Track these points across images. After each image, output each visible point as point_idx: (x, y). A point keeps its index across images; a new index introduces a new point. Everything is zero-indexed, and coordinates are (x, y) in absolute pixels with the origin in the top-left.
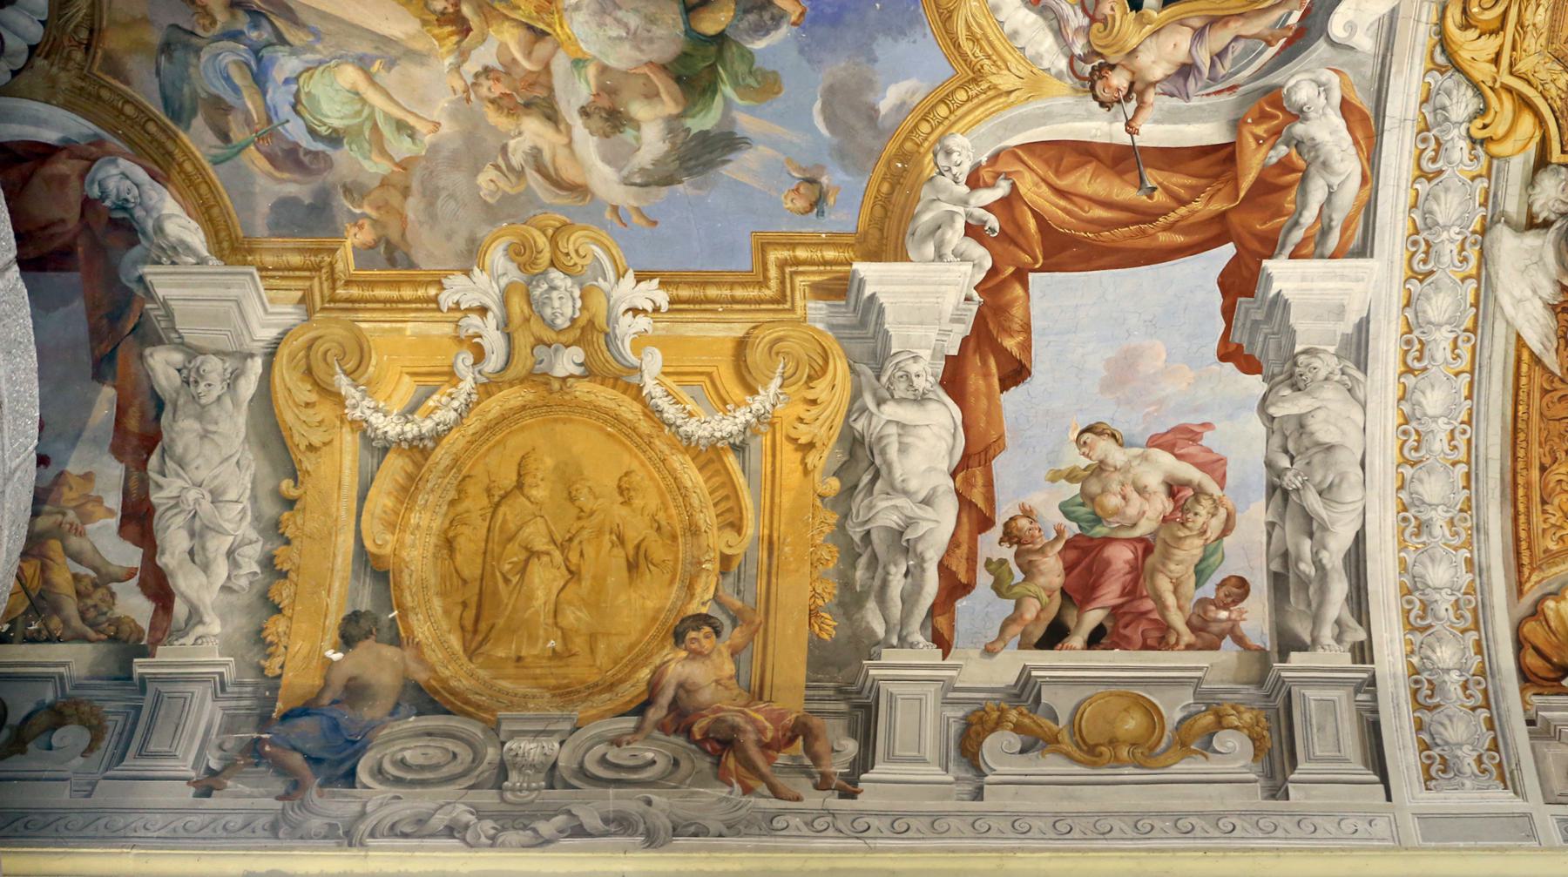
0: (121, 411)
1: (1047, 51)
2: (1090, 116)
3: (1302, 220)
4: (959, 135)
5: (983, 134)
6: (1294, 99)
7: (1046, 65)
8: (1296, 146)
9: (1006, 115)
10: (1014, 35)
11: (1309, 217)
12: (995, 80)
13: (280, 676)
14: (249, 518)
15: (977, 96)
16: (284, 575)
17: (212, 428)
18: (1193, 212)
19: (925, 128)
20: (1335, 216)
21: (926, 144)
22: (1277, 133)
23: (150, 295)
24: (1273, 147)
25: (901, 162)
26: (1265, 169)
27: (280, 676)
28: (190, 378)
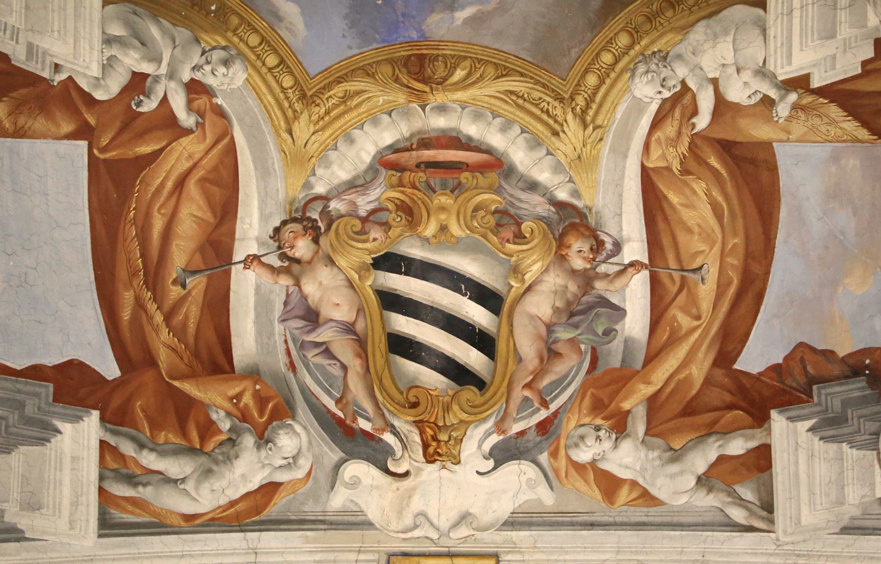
1: (333, 173)
3: (145, 452)
4: (245, 76)
5: (246, 102)
6: (281, 432)
7: (320, 172)
8: (230, 439)
9: (267, 129)
10: (351, 141)
11: (150, 460)
12: (304, 117)
15: (287, 98)
19: (254, 40)
20: (149, 489)
21: (236, 39)
24: (229, 414)
25: (215, 12)
26: (203, 407)
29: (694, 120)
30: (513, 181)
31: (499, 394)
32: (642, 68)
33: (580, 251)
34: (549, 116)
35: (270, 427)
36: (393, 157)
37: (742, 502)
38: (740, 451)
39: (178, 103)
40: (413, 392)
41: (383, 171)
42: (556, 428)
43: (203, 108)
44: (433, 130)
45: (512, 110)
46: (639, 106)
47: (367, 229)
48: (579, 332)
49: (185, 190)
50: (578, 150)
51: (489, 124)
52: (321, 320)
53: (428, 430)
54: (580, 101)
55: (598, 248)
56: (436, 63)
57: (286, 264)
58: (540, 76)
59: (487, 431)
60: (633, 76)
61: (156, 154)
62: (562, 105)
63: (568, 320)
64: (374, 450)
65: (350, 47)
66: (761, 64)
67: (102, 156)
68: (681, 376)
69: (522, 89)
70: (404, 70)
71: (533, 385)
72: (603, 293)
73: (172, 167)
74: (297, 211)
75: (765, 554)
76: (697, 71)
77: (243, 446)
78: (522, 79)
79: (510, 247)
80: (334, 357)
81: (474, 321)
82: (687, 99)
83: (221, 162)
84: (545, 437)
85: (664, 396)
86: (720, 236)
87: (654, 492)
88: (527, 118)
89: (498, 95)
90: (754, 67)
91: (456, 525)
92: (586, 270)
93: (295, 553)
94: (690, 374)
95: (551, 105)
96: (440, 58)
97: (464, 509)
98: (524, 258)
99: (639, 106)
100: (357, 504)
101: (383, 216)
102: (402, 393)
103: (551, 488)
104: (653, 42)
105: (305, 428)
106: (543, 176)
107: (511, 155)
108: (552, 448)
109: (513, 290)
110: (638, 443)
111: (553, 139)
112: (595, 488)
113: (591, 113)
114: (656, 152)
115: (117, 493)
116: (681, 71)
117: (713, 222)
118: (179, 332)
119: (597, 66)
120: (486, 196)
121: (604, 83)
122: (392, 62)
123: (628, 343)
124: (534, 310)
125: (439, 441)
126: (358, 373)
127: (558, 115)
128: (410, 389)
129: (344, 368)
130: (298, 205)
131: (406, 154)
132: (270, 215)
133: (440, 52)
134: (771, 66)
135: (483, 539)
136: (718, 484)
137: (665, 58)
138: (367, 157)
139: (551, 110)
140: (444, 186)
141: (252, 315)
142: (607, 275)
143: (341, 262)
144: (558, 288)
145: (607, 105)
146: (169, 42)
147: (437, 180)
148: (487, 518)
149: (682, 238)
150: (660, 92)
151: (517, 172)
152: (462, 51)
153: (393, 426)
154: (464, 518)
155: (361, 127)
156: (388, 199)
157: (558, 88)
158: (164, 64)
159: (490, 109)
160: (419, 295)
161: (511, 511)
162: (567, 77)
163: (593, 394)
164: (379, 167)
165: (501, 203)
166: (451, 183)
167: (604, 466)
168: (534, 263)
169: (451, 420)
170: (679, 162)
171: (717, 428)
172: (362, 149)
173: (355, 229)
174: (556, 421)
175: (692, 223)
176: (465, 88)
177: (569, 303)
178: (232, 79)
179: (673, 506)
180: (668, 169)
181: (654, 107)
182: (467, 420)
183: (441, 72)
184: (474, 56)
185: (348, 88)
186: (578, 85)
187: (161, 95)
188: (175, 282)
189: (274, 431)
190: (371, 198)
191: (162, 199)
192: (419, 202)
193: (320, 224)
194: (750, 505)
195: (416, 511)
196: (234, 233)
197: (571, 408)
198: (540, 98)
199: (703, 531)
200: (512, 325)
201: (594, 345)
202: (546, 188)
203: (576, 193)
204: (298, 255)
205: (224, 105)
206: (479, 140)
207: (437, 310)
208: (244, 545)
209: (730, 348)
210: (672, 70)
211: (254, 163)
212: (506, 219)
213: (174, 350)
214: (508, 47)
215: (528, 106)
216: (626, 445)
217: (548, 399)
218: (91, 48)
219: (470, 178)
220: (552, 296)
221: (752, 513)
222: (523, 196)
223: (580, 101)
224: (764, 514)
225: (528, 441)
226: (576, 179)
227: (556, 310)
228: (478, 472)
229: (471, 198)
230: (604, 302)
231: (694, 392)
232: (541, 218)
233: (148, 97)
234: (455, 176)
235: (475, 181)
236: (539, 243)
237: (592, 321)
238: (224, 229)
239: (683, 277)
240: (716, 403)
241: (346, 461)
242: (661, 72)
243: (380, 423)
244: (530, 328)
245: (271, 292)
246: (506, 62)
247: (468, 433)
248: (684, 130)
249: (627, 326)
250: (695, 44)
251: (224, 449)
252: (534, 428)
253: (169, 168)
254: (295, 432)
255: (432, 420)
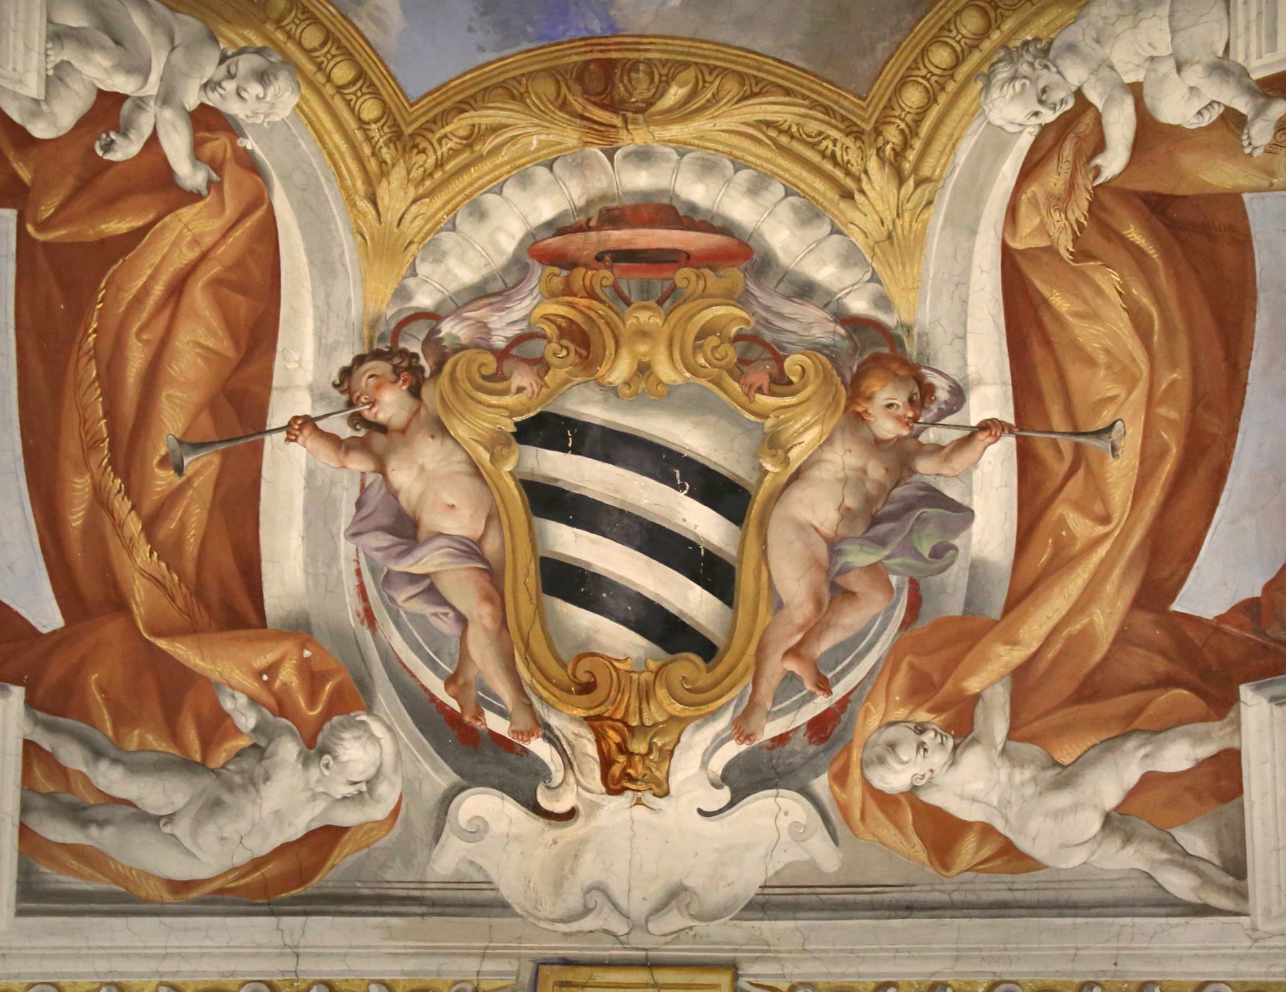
1: (448, 271)
2: (324, 351)
3: (104, 765)
4: (295, 100)
5: (297, 146)
6: (346, 735)
7: (424, 269)
8: (255, 746)
9: (331, 193)
10: (480, 214)
11: (111, 779)
12: (398, 174)
15: (369, 139)
18: (129, 547)
20: (110, 831)
21: (280, 36)
22: (282, 707)
24: (254, 701)
26: (209, 687)
29: (1098, 161)
30: (770, 282)
31: (740, 667)
32: (1003, 72)
33: (890, 406)
34: (836, 164)
35: (327, 726)
36: (555, 242)
37: (1187, 860)
38: (1185, 765)
39: (177, 147)
40: (585, 664)
41: (537, 269)
42: (844, 729)
43: (220, 156)
44: (627, 193)
45: (769, 155)
46: (999, 140)
47: (506, 370)
48: (887, 552)
49: (186, 300)
50: (889, 225)
51: (728, 181)
52: (422, 534)
53: (611, 733)
54: (892, 135)
55: (923, 398)
56: (633, 75)
57: (362, 433)
58: (820, 94)
59: (718, 735)
60: (987, 87)
61: (137, 235)
62: (859, 144)
63: (867, 531)
64: (512, 770)
65: (481, 49)
66: (1220, 54)
67: (41, 237)
68: (1076, 627)
69: (786, 116)
70: (577, 88)
71: (803, 651)
72: (931, 481)
73: (164, 257)
74: (382, 338)
75: (1232, 957)
76: (1105, 73)
77: (278, 759)
78: (787, 99)
79: (764, 400)
80: (444, 602)
81: (696, 535)
82: (1088, 119)
83: (251, 251)
84: (822, 747)
85: (1042, 665)
86: (1145, 369)
87: (1023, 844)
88: (797, 169)
89: (744, 129)
90: (1207, 58)
91: (660, 909)
92: (900, 439)
93: (369, 956)
94: (1091, 623)
95: (839, 145)
96: (642, 67)
97: (675, 879)
98: (789, 420)
99: (999, 140)
100: (480, 869)
101: (535, 348)
102: (564, 666)
103: (835, 838)
104: (1024, 24)
105: (390, 729)
106: (825, 272)
107: (767, 236)
108: (837, 766)
109: (769, 478)
110: (995, 754)
111: (843, 205)
112: (916, 839)
113: (912, 156)
114: (1027, 223)
115: (52, 837)
116: (1075, 74)
117: (1132, 344)
118: (170, 552)
119: (924, 72)
120: (720, 311)
121: (935, 101)
122: (555, 74)
123: (977, 570)
124: (805, 514)
125: (630, 755)
126: (485, 629)
127: (853, 161)
128: (580, 658)
129: (462, 621)
130: (386, 327)
131: (579, 238)
132: (335, 346)
133: (642, 56)
134: (1238, 56)
135: (708, 936)
136: (1144, 827)
137: (1045, 52)
138: (509, 245)
139: (838, 153)
140: (645, 293)
141: (298, 523)
142: (937, 448)
143: (460, 430)
144: (850, 474)
145: (941, 140)
146: (163, 40)
147: (633, 283)
148: (716, 897)
149: (1076, 373)
150: (1036, 114)
151: (777, 265)
152: (681, 53)
153: (548, 727)
154: (675, 895)
155: (499, 190)
156: (545, 318)
157: (852, 112)
158: (154, 77)
159: (731, 154)
160: (599, 489)
161: (761, 883)
162: (868, 93)
163: (912, 667)
164: (529, 261)
165: (747, 322)
166: (659, 288)
167: (932, 798)
168: (807, 428)
169: (654, 714)
170: (1070, 237)
171: (1137, 724)
172: (499, 228)
173: (486, 371)
174: (844, 717)
175: (1094, 347)
176: (685, 118)
177: (869, 501)
178: (273, 105)
179: (1059, 870)
180: (1052, 250)
181: (1026, 141)
182: (682, 715)
183: (642, 89)
184: (702, 61)
185: (477, 121)
186: (889, 106)
187: (147, 132)
188: (163, 462)
189: (335, 734)
190: (516, 315)
191: (145, 315)
192: (601, 322)
193: (423, 362)
194: (1202, 866)
195: (588, 883)
196: (270, 377)
197: (870, 694)
198: (820, 133)
199: (1116, 916)
200: (765, 543)
201: (916, 576)
202: (829, 293)
203: (883, 302)
204: (382, 417)
205: (258, 151)
206: (709, 211)
207: (630, 515)
208: (276, 939)
209: (1165, 573)
210: (1059, 73)
211: (309, 252)
212: (757, 351)
213: (159, 583)
214: (763, 43)
215: (798, 147)
216: (973, 759)
217: (829, 676)
218: (28, 48)
219: (693, 278)
220: (839, 487)
221: (1206, 880)
222: (788, 308)
223: (892, 135)
224: (1229, 880)
225: (792, 753)
226: (884, 275)
227: (847, 514)
228: (700, 812)
229: (694, 315)
230: (934, 497)
231: (1098, 657)
232: (819, 348)
233: (125, 134)
234: (667, 274)
235: (701, 283)
236: (814, 393)
237: (911, 530)
238: (253, 369)
239: (1078, 448)
240: (1141, 676)
241: (463, 789)
242: (1038, 78)
243: (524, 721)
244: (798, 546)
245: (333, 483)
246: (760, 70)
247: (683, 739)
248: (1080, 180)
249: (974, 540)
250: (1101, 23)
251: (245, 764)
252: (804, 729)
253: (157, 260)
254: (372, 736)
255: (619, 716)
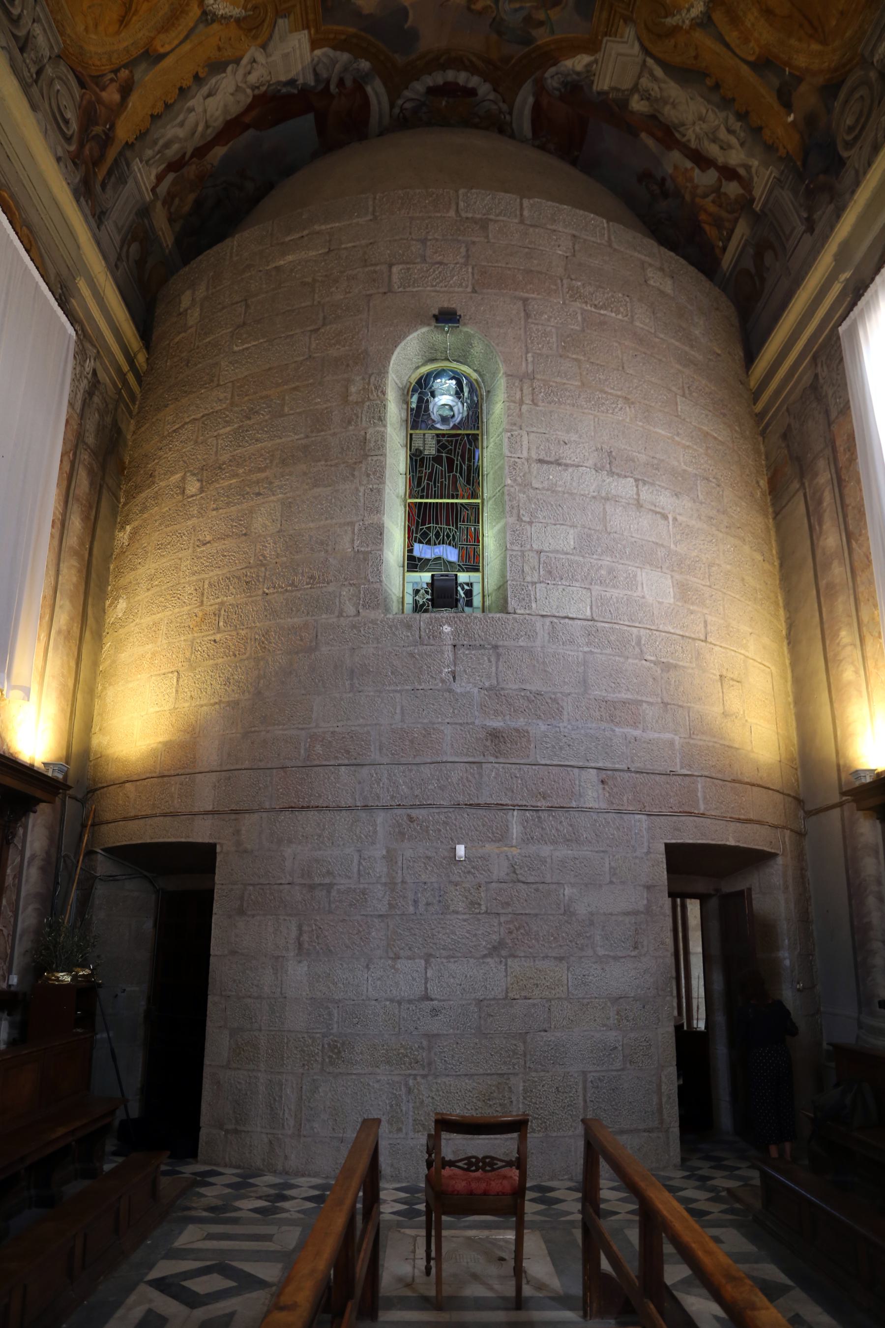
0: (652, 135)
13: (788, 152)
14: (717, 111)
16: (747, 113)
17: (671, 100)
23: (606, 93)
27: (788, 152)
28: (646, 96)
